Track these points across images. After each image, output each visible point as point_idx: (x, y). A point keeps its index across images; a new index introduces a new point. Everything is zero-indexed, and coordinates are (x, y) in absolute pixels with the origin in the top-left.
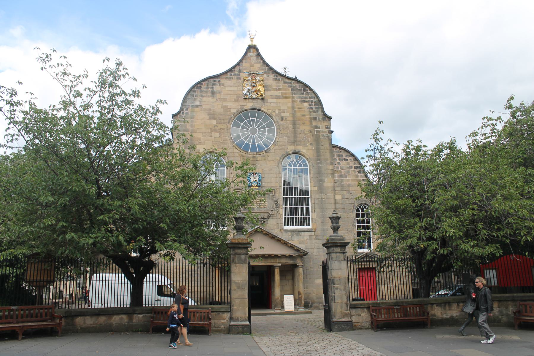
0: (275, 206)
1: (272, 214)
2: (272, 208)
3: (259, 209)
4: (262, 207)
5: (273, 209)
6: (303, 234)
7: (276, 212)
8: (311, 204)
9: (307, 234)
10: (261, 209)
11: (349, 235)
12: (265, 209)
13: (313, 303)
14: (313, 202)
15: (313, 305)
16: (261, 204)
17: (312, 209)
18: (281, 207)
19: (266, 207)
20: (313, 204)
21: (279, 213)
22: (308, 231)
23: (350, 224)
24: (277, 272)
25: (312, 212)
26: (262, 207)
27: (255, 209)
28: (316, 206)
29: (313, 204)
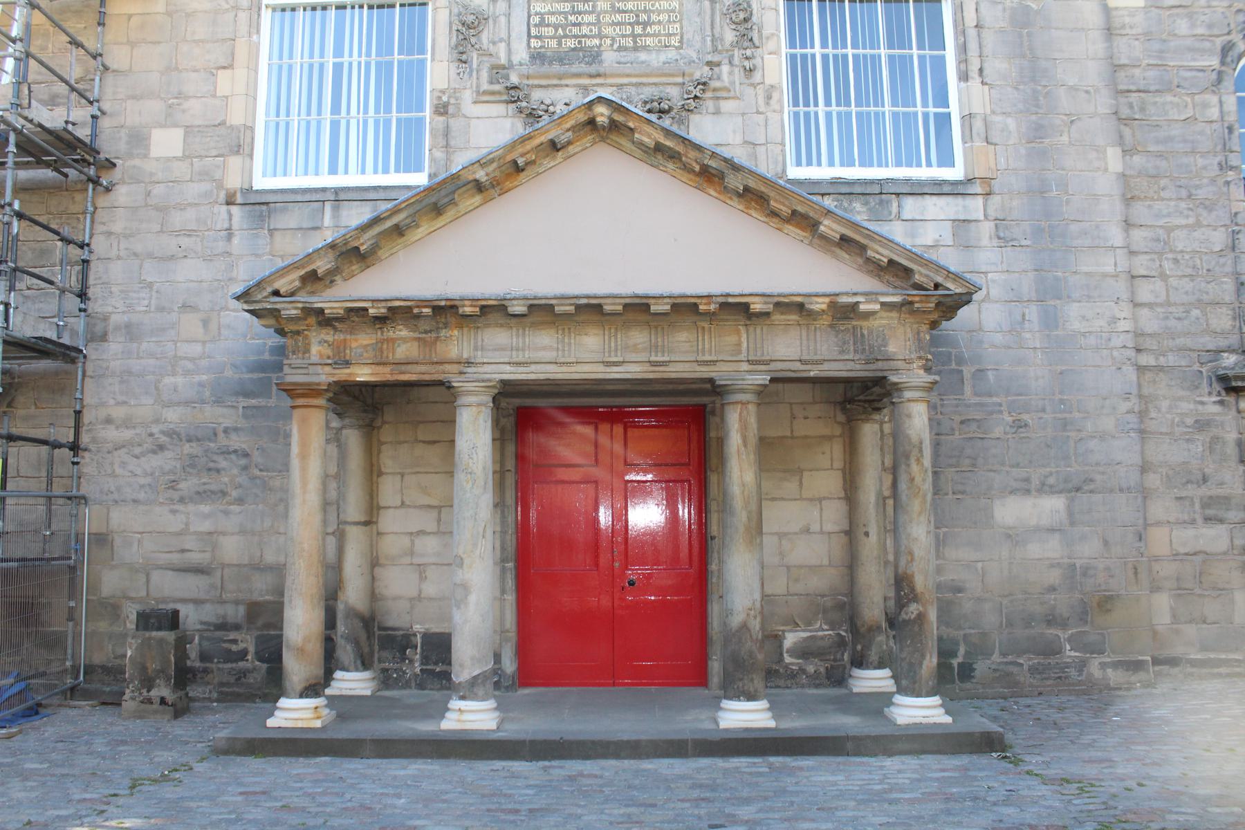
0: (730, 36)
1: (714, 84)
2: (715, 50)
3: (631, 56)
4: (649, 41)
5: (716, 58)
6: (911, 206)
7: (738, 74)
8: (960, 30)
9: (937, 208)
10: (643, 56)
11: (1198, 224)
12: (672, 54)
13: (980, 649)
14: (970, 18)
15: (981, 668)
16: (645, 24)
17: (963, 59)
18: (771, 45)
19: (675, 41)
20: (972, 33)
21: (757, 77)
22: (939, 189)
23: (1201, 162)
24: (744, 427)
25: (964, 77)
26: (649, 41)
27: (609, 57)
28: (989, 38)
29: (972, 33)
